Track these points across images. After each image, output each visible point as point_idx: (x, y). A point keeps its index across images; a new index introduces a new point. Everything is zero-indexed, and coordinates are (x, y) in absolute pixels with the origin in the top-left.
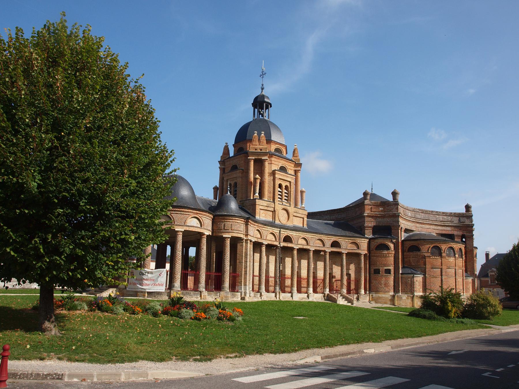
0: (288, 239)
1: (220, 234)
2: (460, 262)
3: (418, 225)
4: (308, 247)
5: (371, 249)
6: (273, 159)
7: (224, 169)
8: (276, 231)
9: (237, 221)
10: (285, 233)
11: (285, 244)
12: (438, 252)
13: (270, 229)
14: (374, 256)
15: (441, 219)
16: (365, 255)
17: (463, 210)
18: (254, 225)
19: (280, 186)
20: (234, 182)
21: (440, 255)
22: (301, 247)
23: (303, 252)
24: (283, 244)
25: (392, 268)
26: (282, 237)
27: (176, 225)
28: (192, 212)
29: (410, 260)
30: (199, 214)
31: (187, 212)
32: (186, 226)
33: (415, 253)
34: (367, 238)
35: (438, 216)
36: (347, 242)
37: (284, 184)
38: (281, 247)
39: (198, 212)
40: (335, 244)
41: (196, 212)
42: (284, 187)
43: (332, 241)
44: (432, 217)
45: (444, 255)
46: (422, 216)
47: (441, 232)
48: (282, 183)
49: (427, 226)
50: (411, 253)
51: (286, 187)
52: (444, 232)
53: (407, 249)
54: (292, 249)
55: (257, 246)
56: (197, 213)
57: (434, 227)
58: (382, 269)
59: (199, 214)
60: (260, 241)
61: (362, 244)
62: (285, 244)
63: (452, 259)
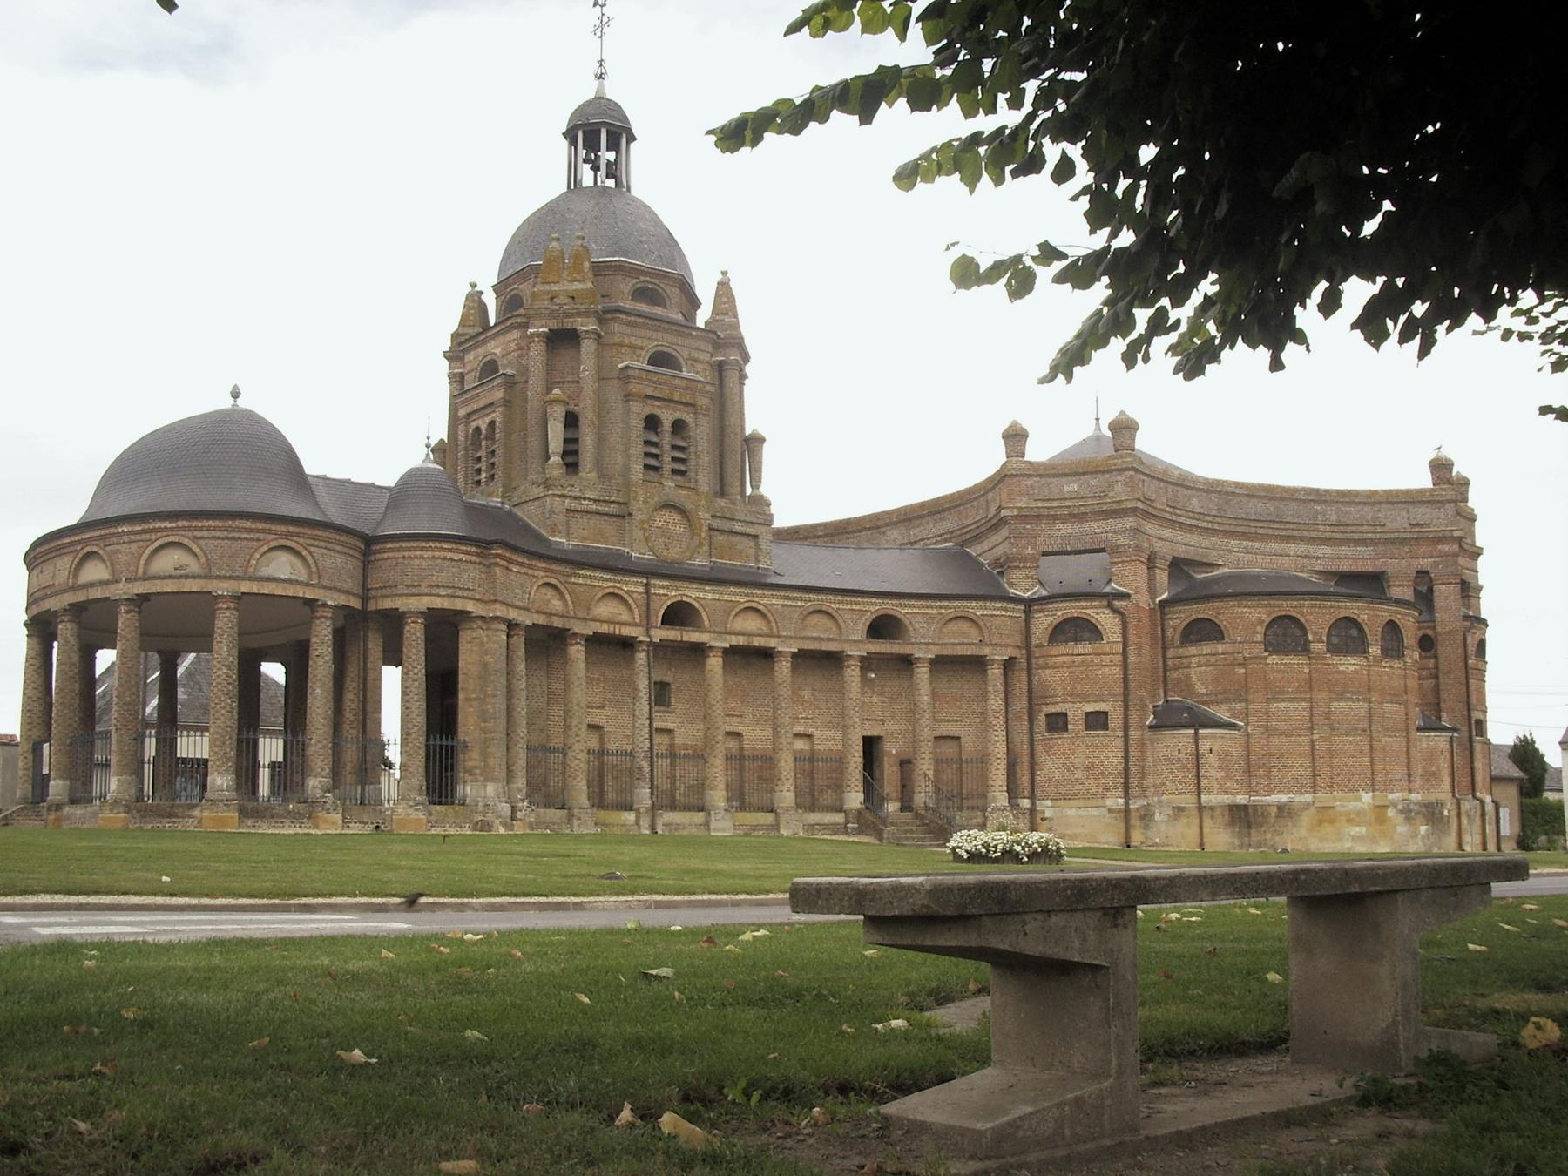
0: (678, 615)
1: (387, 604)
2: (1403, 671)
4: (772, 643)
5: (1035, 642)
6: (615, 327)
7: (462, 375)
8: (632, 586)
9: (449, 555)
10: (667, 593)
11: (672, 634)
12: (1286, 635)
13: (606, 581)
14: (1047, 667)
15: (1334, 518)
16: (1008, 665)
17: (1424, 481)
18: (530, 567)
19: (652, 423)
20: (488, 420)
21: (1303, 648)
22: (741, 641)
24: (660, 634)
25: (1112, 707)
27: (219, 577)
28: (270, 532)
29: (1188, 676)
30: (298, 535)
31: (251, 531)
32: (251, 579)
33: (1208, 648)
34: (1017, 600)
36: (932, 617)
37: (667, 417)
38: (651, 643)
39: (292, 529)
41: (283, 528)
42: (667, 425)
43: (869, 618)
45: (1318, 647)
47: (1333, 566)
48: (657, 412)
49: (1274, 547)
50: (1193, 650)
51: (678, 426)
52: (1345, 567)
53: (1178, 636)
55: (546, 643)
56: (292, 534)
57: (1303, 548)
58: (1076, 712)
59: (298, 535)
60: (557, 623)
61: (997, 622)
62: (672, 634)
63: (1349, 665)
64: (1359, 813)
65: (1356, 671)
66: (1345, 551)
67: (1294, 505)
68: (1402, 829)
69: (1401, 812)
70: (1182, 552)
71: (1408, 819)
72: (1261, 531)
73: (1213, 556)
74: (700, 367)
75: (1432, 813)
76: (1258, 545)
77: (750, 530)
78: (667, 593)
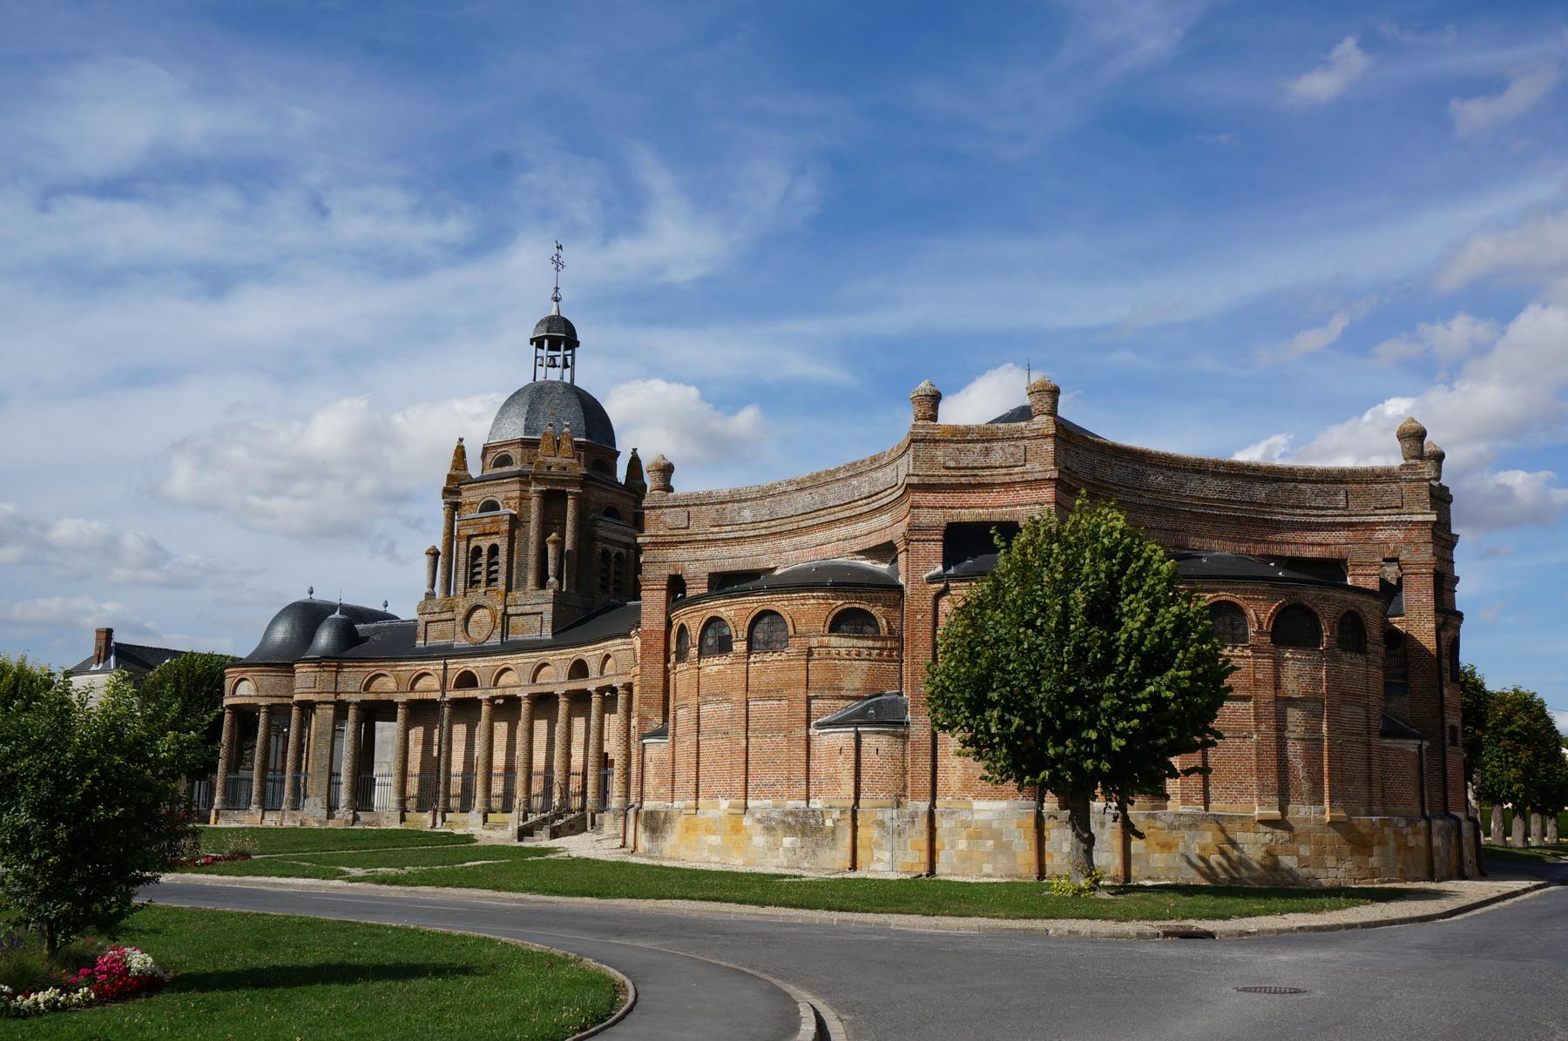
3: (785, 543)
10: (457, 666)
15: (866, 491)
19: (478, 550)
23: (507, 708)
24: (451, 695)
26: (452, 678)
35: (855, 482)
40: (579, 670)
44: (835, 494)
46: (803, 501)
49: (820, 536)
51: (494, 550)
54: (476, 703)
62: (459, 694)
63: (714, 666)
64: (715, 821)
65: (719, 672)
66: (862, 527)
67: (836, 487)
68: (759, 840)
69: (759, 821)
70: (727, 566)
71: (769, 830)
72: (803, 524)
73: (765, 562)
74: (512, 503)
75: (805, 826)
76: (805, 538)
77: (538, 610)
78: (457, 666)
